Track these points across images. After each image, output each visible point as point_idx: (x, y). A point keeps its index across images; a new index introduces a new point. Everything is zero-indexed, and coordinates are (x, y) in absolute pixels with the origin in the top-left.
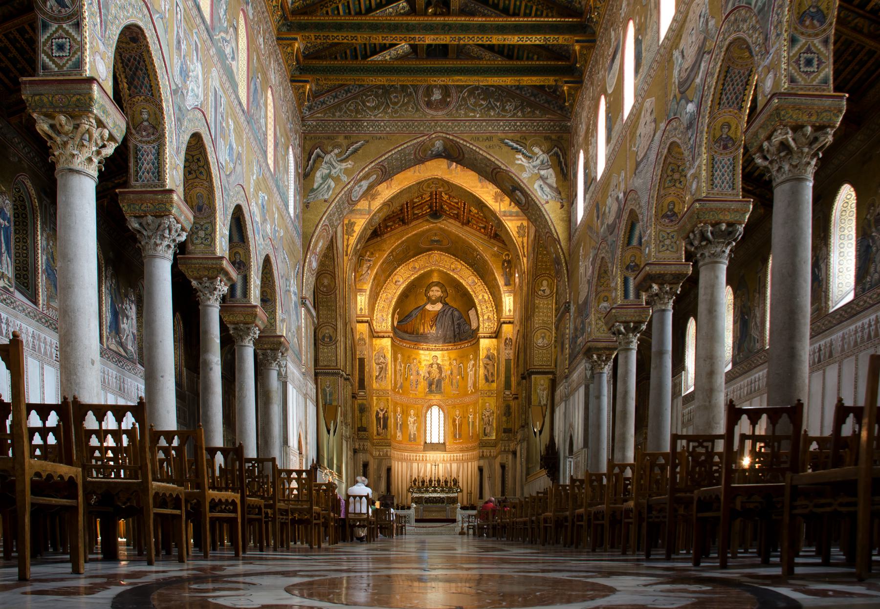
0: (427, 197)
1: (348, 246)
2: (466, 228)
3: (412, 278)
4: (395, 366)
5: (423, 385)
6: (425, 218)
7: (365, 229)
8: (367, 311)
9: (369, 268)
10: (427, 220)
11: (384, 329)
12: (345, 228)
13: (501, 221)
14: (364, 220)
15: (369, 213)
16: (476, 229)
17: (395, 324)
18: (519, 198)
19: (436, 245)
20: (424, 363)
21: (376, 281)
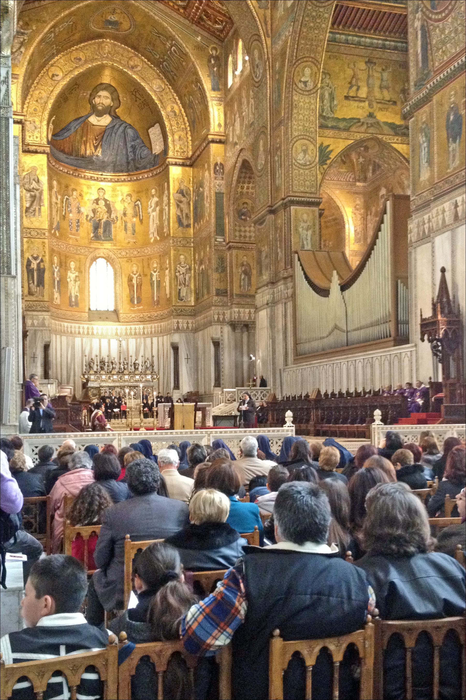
3: (76, 73)
5: (87, 227)
16: (172, 8)
19: (111, 30)
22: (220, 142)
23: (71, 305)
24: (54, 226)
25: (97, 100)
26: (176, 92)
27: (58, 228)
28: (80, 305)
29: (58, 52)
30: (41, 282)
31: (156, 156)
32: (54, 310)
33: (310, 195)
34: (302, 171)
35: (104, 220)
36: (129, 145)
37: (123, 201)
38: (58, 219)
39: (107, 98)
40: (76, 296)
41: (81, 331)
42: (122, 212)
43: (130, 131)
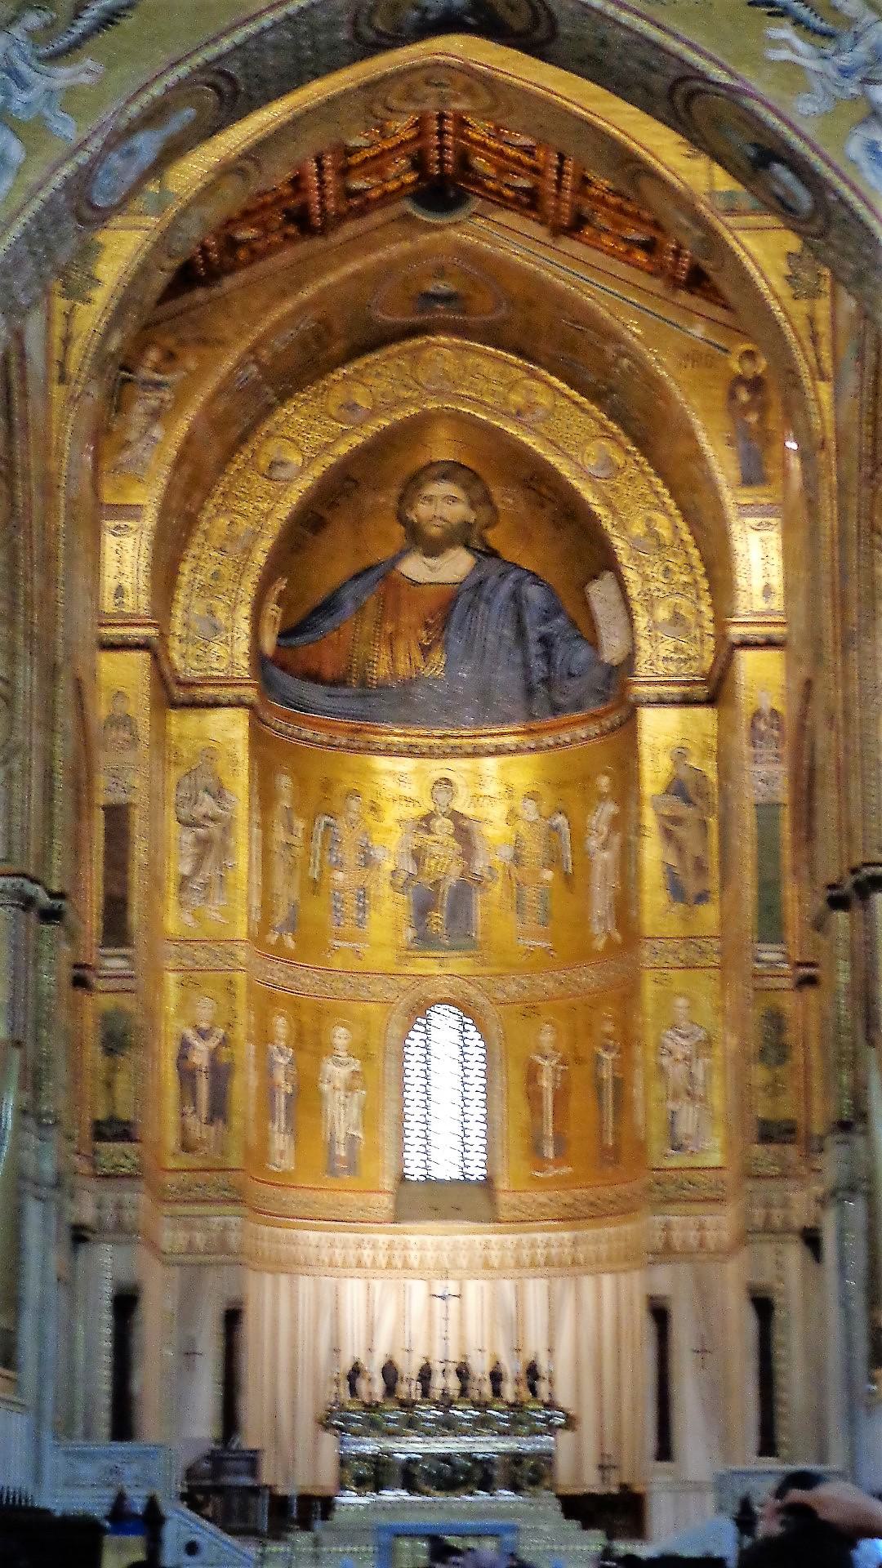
0: (401, 127)
1: (67, 341)
2: (568, 245)
3: (343, 449)
6: (393, 211)
7: (143, 271)
8: (144, 599)
10: (406, 217)
11: (219, 668)
17: (269, 643)
18: (784, 186)
19: (441, 312)
20: (393, 813)
21: (187, 470)
22: (769, 643)
23: (332, 1172)
24: (279, 920)
25: (422, 511)
27: (292, 924)
29: (284, 397)
30: (219, 1110)
35: (452, 881)
36: (532, 635)
38: (295, 896)
39: (454, 500)
40: (352, 1140)
41: (367, 1254)
42: (508, 852)
43: (533, 593)
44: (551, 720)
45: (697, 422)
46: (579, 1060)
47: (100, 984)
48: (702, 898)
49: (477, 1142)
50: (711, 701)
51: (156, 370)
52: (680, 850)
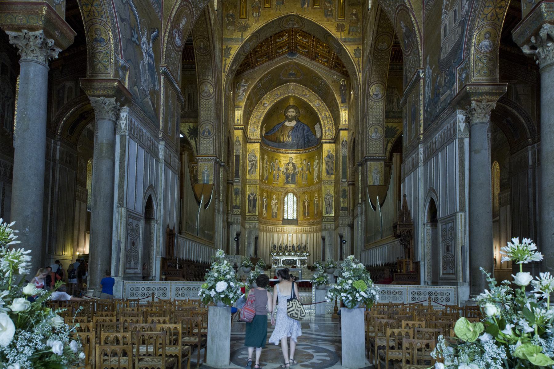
1: (225, 65)
2: (313, 62)
3: (275, 101)
4: (263, 164)
5: (282, 178)
6: (284, 56)
7: (238, 54)
8: (242, 121)
9: (244, 91)
11: (255, 137)
12: (224, 52)
13: (342, 46)
14: (238, 46)
15: (242, 41)
17: (263, 134)
20: (283, 162)
22: (345, 129)
23: (272, 217)
25: (289, 114)
26: (327, 105)
27: (267, 179)
28: (278, 217)
30: (255, 206)
31: (318, 139)
32: (263, 219)
33: (379, 155)
34: (374, 142)
36: (305, 135)
37: (302, 163)
39: (293, 112)
40: (276, 213)
42: (301, 169)
44: (308, 148)
45: (334, 93)
46: (311, 201)
47: (234, 184)
48: (332, 174)
49: (295, 213)
50: (334, 143)
51: (244, 83)
52: (329, 166)
